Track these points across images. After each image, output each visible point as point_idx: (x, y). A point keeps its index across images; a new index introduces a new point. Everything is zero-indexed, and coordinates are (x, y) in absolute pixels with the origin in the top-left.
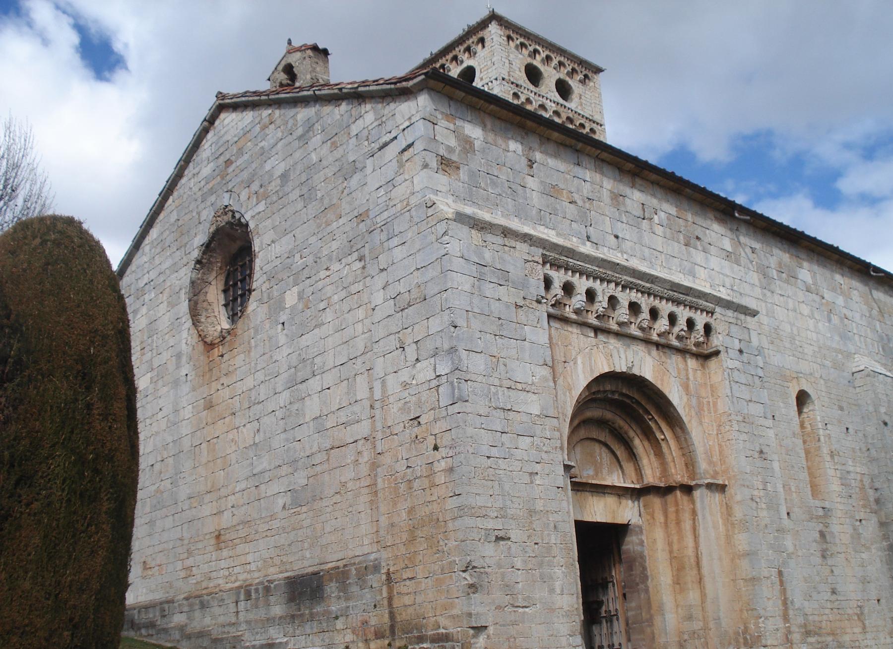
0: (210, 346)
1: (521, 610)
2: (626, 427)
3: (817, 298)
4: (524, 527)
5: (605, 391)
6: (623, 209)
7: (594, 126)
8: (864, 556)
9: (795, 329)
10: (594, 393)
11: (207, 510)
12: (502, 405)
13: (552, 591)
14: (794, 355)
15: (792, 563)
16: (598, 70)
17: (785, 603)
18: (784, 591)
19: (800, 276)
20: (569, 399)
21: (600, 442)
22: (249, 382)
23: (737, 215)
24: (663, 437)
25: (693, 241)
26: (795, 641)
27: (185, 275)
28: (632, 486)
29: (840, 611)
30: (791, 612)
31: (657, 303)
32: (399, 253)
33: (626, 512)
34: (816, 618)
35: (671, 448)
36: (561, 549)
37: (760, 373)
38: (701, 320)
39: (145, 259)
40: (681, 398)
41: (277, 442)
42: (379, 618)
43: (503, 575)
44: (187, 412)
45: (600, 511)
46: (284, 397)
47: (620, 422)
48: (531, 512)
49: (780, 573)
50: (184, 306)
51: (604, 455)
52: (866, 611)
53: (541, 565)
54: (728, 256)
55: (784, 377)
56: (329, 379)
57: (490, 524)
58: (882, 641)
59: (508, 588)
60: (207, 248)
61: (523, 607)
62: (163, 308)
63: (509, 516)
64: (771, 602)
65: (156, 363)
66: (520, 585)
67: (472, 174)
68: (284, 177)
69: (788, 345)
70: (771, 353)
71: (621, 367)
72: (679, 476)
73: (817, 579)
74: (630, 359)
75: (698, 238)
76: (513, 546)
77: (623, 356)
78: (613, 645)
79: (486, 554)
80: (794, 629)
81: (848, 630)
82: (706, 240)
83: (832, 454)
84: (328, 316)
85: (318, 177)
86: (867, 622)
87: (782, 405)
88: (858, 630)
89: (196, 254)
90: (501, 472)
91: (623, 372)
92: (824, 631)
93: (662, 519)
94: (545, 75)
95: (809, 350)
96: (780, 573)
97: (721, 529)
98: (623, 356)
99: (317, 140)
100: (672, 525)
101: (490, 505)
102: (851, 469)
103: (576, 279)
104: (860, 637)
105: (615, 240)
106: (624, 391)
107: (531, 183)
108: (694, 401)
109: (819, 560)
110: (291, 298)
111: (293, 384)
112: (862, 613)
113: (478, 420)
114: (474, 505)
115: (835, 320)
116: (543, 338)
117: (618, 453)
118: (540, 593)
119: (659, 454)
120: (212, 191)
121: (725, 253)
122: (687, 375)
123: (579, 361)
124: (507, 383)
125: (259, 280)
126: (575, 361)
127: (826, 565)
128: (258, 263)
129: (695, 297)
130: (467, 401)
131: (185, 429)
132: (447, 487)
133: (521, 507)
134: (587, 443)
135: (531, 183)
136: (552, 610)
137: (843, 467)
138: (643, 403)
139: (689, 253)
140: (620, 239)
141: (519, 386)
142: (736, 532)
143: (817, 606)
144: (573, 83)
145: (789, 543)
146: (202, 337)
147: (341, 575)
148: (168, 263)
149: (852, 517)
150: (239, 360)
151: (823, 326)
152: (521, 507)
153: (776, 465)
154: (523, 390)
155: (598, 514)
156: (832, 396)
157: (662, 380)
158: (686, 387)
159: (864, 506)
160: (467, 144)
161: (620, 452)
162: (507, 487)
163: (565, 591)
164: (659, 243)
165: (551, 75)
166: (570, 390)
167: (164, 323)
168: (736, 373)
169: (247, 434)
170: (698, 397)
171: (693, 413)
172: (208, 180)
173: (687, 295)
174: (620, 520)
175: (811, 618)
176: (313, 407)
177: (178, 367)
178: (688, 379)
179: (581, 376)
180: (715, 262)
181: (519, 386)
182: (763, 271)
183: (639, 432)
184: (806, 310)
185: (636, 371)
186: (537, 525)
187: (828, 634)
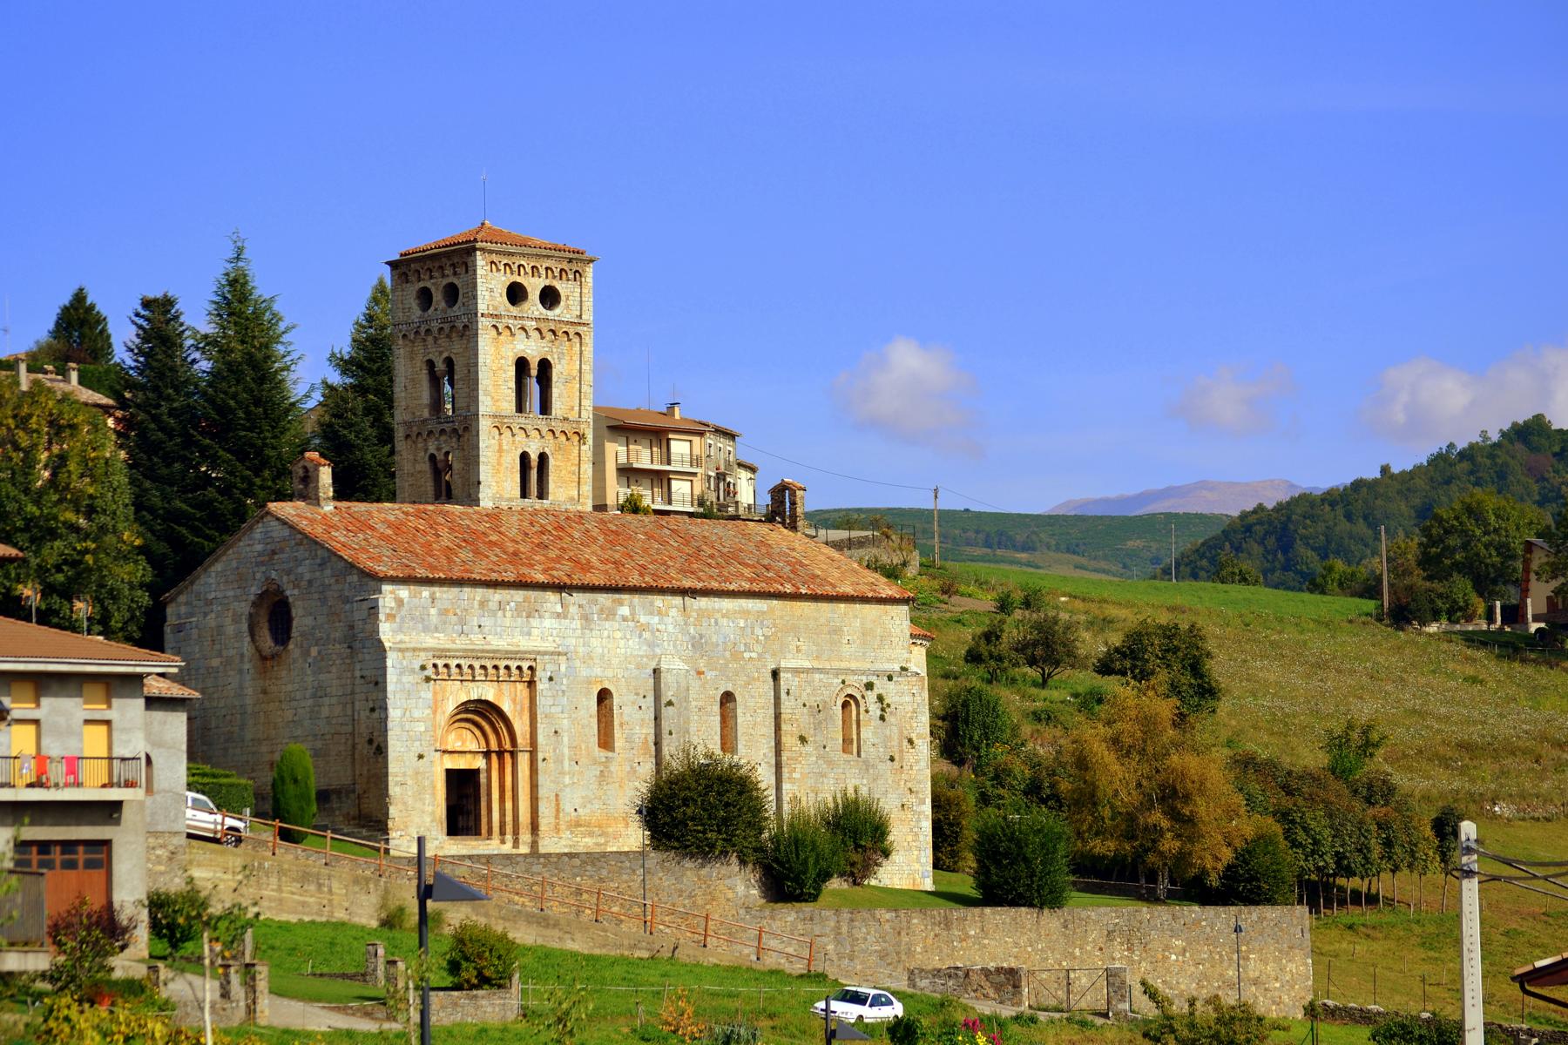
0: (264, 658)
7: (580, 329)
11: (264, 749)
17: (558, 811)
22: (290, 687)
27: (244, 608)
32: (367, 657)
33: (479, 763)
38: (525, 665)
39: (211, 581)
41: (306, 723)
42: (354, 812)
44: (250, 691)
45: (462, 763)
46: (310, 702)
50: (245, 627)
54: (559, 615)
56: (334, 700)
59: (405, 803)
60: (261, 596)
62: (228, 621)
65: (224, 653)
67: (402, 618)
68: (310, 582)
83: (621, 725)
84: (334, 669)
85: (329, 594)
89: (252, 598)
94: (529, 290)
95: (615, 661)
99: (328, 572)
107: (433, 611)
110: (314, 651)
111: (314, 696)
116: (430, 695)
118: (418, 805)
120: (263, 564)
125: (295, 633)
128: (295, 623)
131: (249, 701)
135: (433, 611)
146: (258, 650)
147: (338, 792)
148: (230, 593)
150: (284, 673)
151: (633, 642)
158: (514, 701)
160: (400, 602)
161: (478, 733)
164: (507, 622)
165: (534, 286)
167: (230, 629)
169: (289, 714)
172: (260, 554)
176: (325, 711)
177: (242, 661)
180: (548, 622)
182: (586, 618)
184: (618, 635)
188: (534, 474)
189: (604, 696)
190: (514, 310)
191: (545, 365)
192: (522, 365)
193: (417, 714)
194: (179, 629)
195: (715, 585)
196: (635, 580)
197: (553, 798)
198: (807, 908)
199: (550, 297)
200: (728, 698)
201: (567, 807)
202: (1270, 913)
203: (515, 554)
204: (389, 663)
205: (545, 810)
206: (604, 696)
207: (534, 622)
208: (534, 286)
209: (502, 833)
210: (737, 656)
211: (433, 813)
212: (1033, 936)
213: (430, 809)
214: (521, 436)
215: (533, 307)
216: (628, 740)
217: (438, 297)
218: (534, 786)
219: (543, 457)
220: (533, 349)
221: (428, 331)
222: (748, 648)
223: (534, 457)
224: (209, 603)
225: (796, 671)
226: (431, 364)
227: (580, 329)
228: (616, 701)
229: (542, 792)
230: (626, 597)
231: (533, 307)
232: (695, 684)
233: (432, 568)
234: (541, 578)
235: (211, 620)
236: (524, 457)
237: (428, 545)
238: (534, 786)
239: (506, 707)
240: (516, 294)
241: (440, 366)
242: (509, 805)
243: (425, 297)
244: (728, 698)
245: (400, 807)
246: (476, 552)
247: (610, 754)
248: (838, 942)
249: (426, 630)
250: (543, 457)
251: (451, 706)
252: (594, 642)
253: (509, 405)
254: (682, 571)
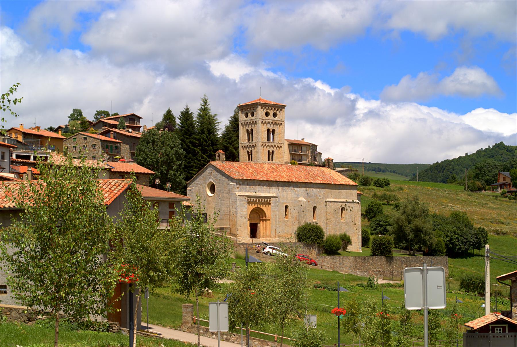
7: (282, 122)
16: (285, 106)
35: (264, 215)
42: (229, 232)
45: (253, 222)
55: (283, 203)
72: (264, 218)
95: (289, 199)
110: (221, 196)
111: (220, 206)
135: (248, 187)
144: (278, 112)
147: (226, 228)
151: (293, 194)
165: (271, 113)
176: (223, 209)
188: (271, 156)
189: (286, 207)
190: (267, 118)
191: (274, 131)
192: (268, 130)
193: (244, 210)
194: (190, 190)
195: (312, 182)
196: (294, 180)
198: (333, 256)
199: (275, 115)
200: (315, 208)
201: (278, 232)
202: (439, 258)
203: (267, 174)
204: (238, 199)
206: (286, 207)
207: (271, 190)
208: (271, 113)
210: (317, 198)
212: (385, 263)
214: (268, 147)
215: (271, 117)
216: (292, 217)
217: (249, 114)
219: (273, 152)
220: (271, 128)
221: (247, 123)
222: (320, 196)
223: (271, 151)
224: (197, 184)
225: (331, 202)
226: (248, 130)
227: (282, 122)
228: (289, 208)
230: (292, 184)
231: (271, 117)
232: (307, 204)
233: (247, 177)
234: (272, 179)
235: (197, 188)
236: (269, 151)
237: (247, 172)
240: (267, 114)
241: (249, 131)
243: (247, 116)
244: (315, 208)
246: (258, 173)
248: (340, 264)
249: (246, 191)
250: (273, 152)
252: (285, 194)
253: (265, 140)
254: (305, 178)
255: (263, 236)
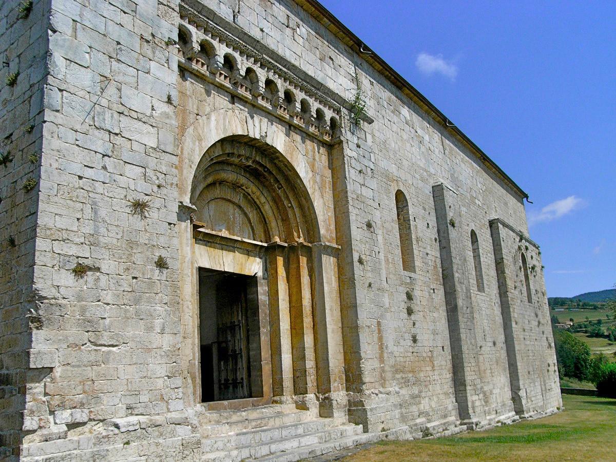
1: (104, 349)
2: (258, 193)
3: (413, 131)
4: (121, 258)
5: (239, 156)
6: (269, 11)
8: (435, 315)
9: (397, 146)
10: (228, 154)
12: (108, 127)
13: (149, 329)
14: (395, 164)
15: (388, 315)
17: (381, 348)
18: (380, 339)
19: (403, 112)
20: (197, 149)
21: (234, 203)
23: (362, 50)
24: (290, 205)
25: (327, 59)
26: (387, 378)
28: (260, 243)
29: (418, 354)
30: (385, 355)
31: (292, 88)
33: (254, 267)
34: (402, 360)
36: (166, 286)
37: (372, 167)
38: (329, 114)
40: (307, 172)
43: (83, 310)
47: (252, 188)
48: (132, 244)
49: (379, 324)
51: (237, 215)
52: (435, 355)
53: (137, 301)
57: (73, 250)
58: (444, 376)
61: (109, 346)
63: (102, 244)
64: (370, 346)
66: (107, 321)
69: (392, 156)
70: (380, 158)
71: (255, 133)
73: (404, 330)
74: (264, 129)
75: (330, 58)
76: (104, 279)
77: (257, 124)
78: (237, 379)
79: (62, 282)
80: (387, 368)
81: (423, 369)
82: (337, 62)
86: (435, 363)
87: (385, 197)
88: (429, 368)
90: (96, 196)
91: (255, 139)
92: (407, 369)
93: (284, 275)
96: (379, 324)
97: (333, 285)
98: (257, 124)
100: (293, 280)
101: (75, 229)
102: (429, 252)
103: (215, 43)
104: (431, 373)
105: (261, 32)
106: (257, 159)
108: (318, 178)
109: (406, 315)
112: (432, 356)
113: (71, 136)
114: (51, 225)
115: (423, 149)
117: (251, 216)
118: (134, 331)
119: (285, 220)
121: (350, 77)
122: (314, 156)
123: (213, 118)
124: (121, 109)
126: (208, 117)
127: (411, 319)
129: (324, 93)
130: (58, 111)
132: (25, 207)
133: (119, 237)
134: (220, 202)
136: (149, 350)
137: (424, 250)
138: (274, 172)
139: (322, 66)
140: (265, 34)
141: (134, 115)
142: (346, 287)
143: (402, 350)
145: (386, 300)
149: (429, 286)
152: (119, 237)
153: (380, 238)
154: (138, 119)
155: (226, 265)
156: (419, 199)
157: (292, 154)
159: (437, 280)
161: (253, 215)
162: (103, 213)
163: (167, 330)
166: (200, 140)
168: (353, 161)
170: (322, 176)
171: (317, 188)
173: (318, 89)
174: (247, 272)
175: (398, 359)
178: (314, 159)
179: (214, 131)
181: (134, 115)
183: (269, 199)
185: (269, 141)
186: (138, 259)
187: (410, 372)
193: (137, 101)
197: (374, 328)
205: (368, 349)
209: (300, 389)
211: (173, 353)
213: (166, 342)
218: (349, 308)
229: (364, 317)
238: (349, 308)
239: (302, 169)
242: (309, 340)
245: (74, 333)
247: (412, 275)
251: (214, 136)
255: (299, 374)
